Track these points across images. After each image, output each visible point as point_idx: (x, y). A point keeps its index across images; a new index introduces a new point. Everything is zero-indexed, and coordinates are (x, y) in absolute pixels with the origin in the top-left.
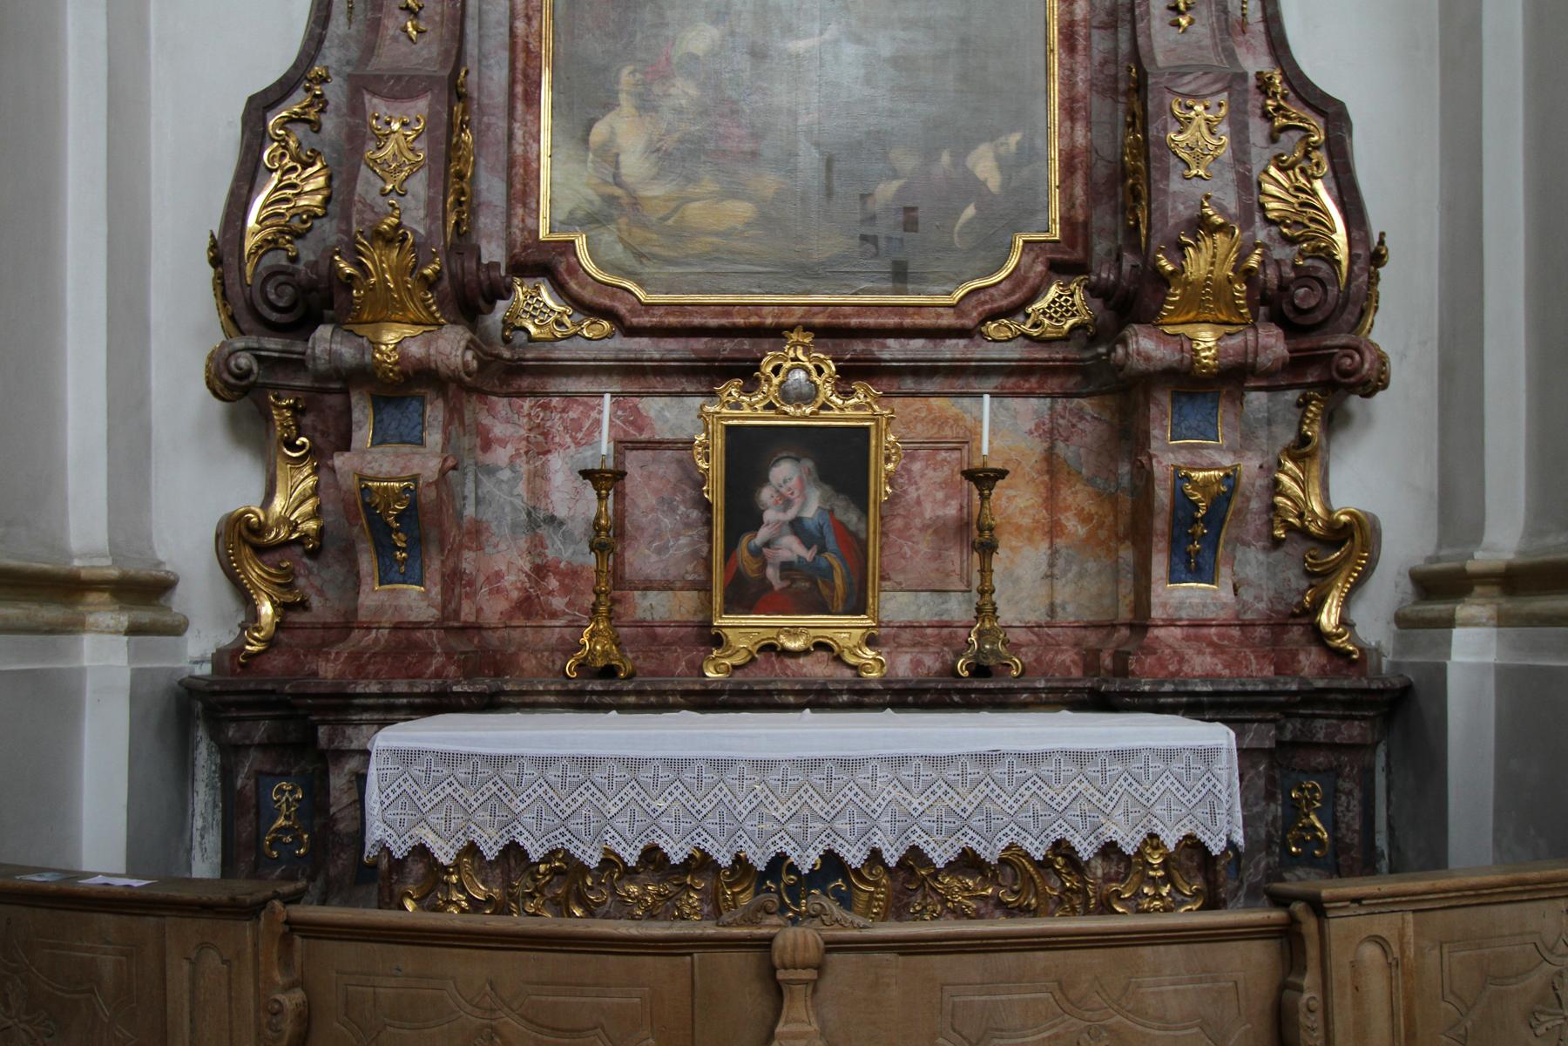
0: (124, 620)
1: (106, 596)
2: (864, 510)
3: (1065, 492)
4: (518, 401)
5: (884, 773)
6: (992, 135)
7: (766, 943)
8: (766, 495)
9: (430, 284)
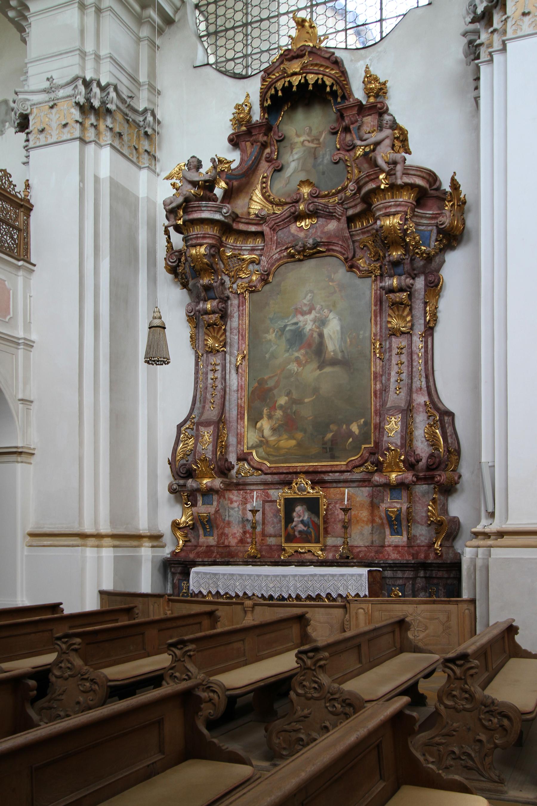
0: (150, 544)
1: (147, 539)
4: (239, 491)
8: (295, 514)
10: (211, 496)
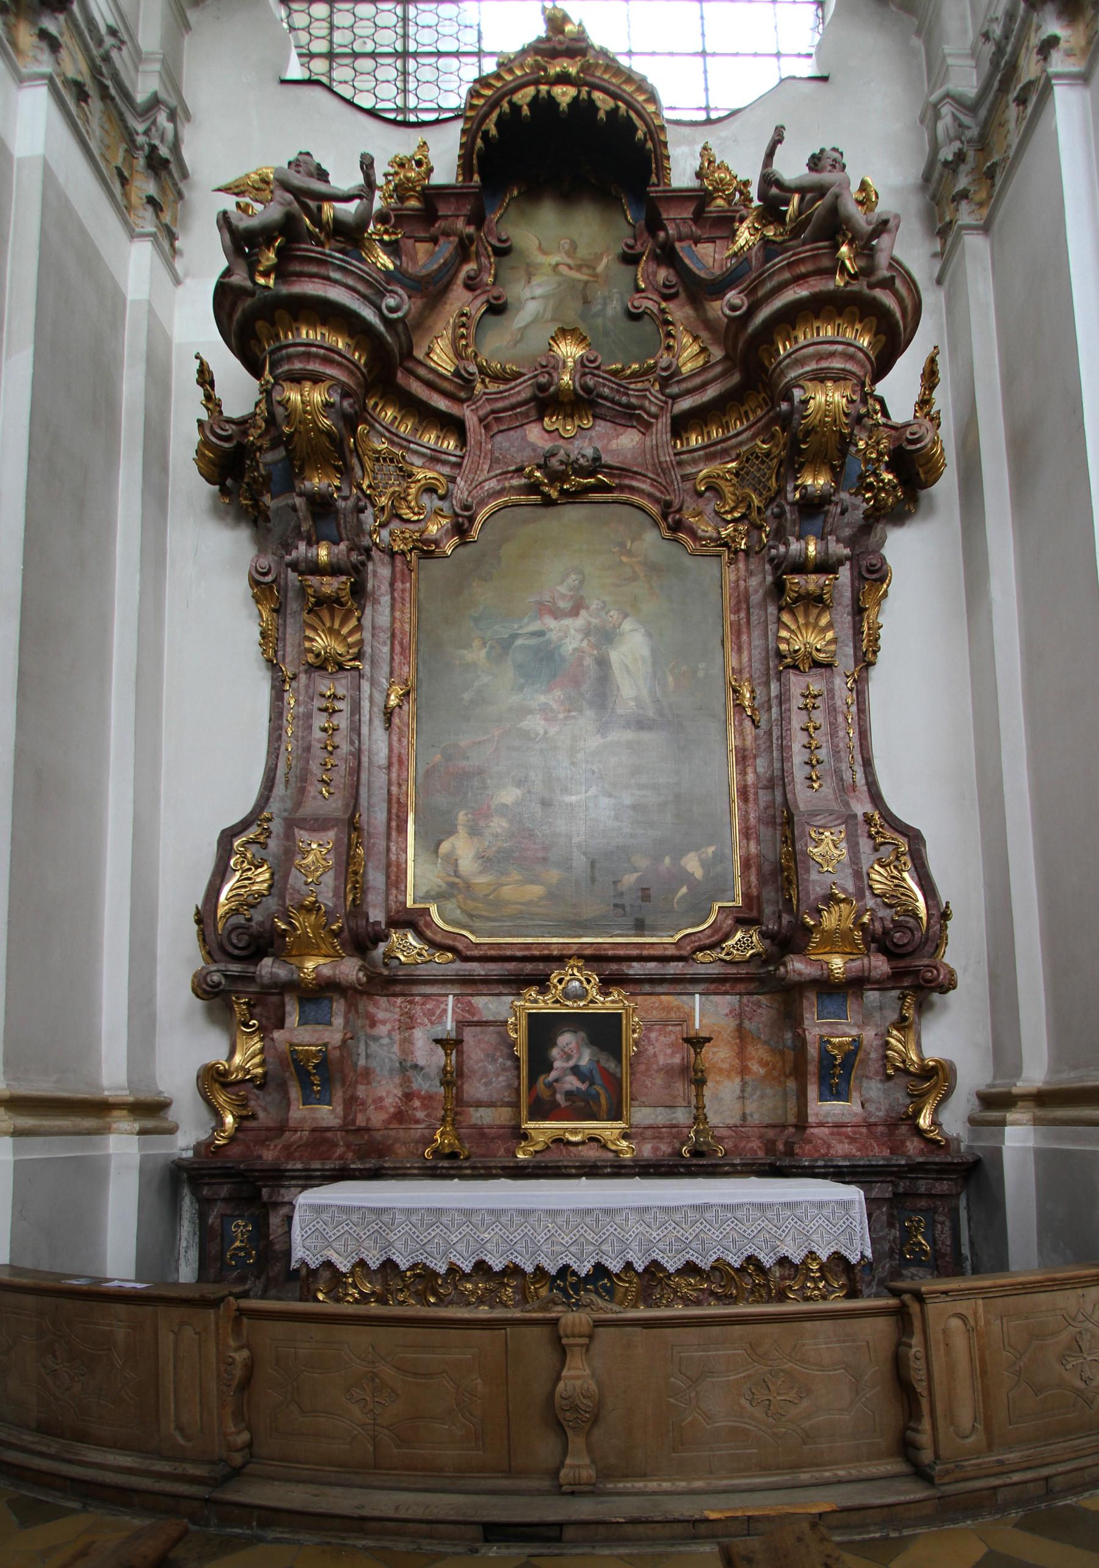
0: (136, 1126)
2: (619, 1060)
3: (751, 1050)
4: (394, 999)
5: (633, 1217)
6: (697, 848)
7: (555, 1322)
8: (555, 1052)
9: (336, 934)
10: (326, 1002)
